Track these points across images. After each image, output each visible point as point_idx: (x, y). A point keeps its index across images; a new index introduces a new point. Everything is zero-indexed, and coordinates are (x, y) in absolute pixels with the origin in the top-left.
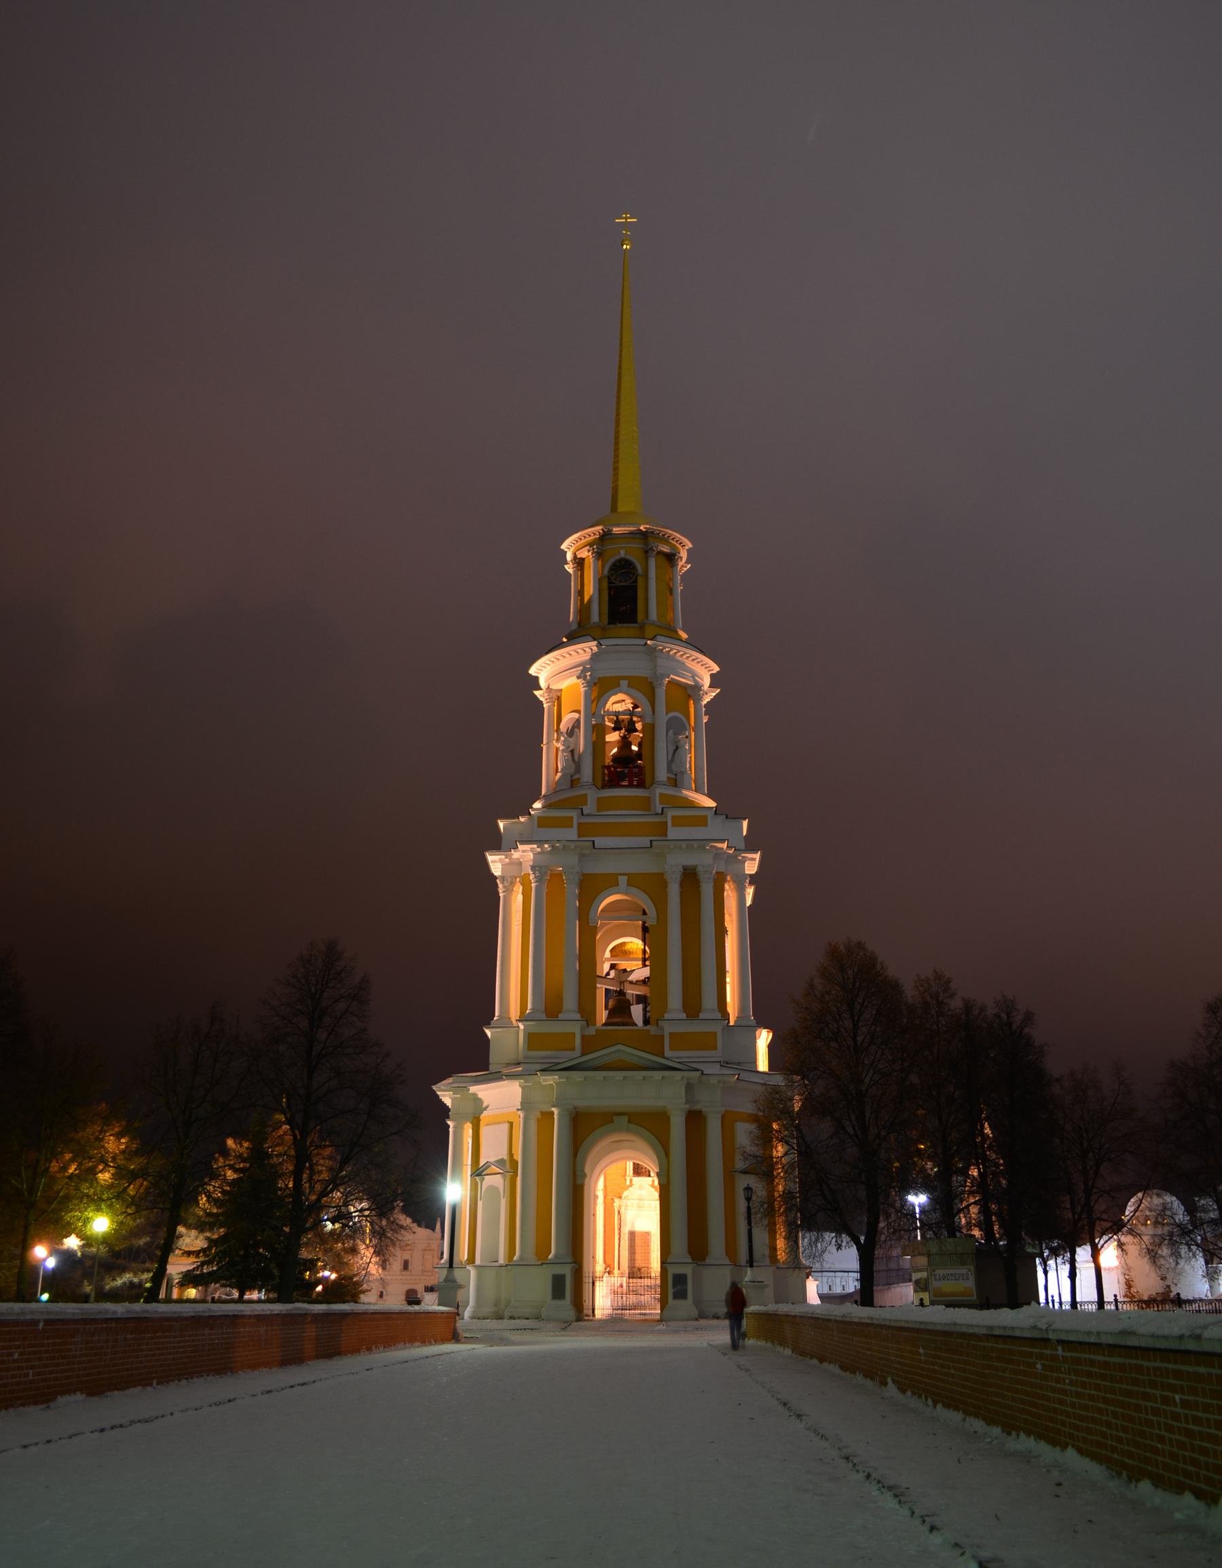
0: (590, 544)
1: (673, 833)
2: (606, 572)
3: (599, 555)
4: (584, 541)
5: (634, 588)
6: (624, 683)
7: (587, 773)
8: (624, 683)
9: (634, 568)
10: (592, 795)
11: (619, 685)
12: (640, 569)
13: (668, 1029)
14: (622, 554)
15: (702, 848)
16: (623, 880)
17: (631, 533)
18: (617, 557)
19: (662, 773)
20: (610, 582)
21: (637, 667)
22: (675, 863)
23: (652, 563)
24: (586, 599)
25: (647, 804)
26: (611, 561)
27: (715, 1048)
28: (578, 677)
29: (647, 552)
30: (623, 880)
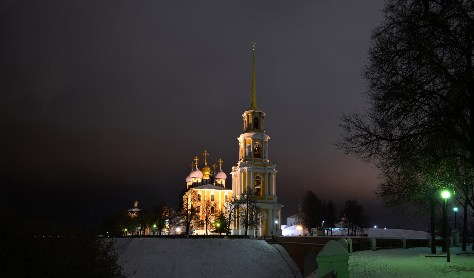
0: (251, 113)
1: (268, 167)
2: (254, 118)
3: (252, 115)
4: (250, 112)
5: (258, 123)
6: (258, 140)
7: (253, 155)
8: (258, 140)
9: (258, 119)
10: (254, 159)
11: (257, 140)
12: (259, 119)
13: (267, 197)
14: (256, 116)
15: (272, 170)
16: (259, 173)
17: (258, 112)
18: (255, 116)
19: (264, 157)
20: (254, 121)
21: (260, 137)
22: (268, 171)
23: (261, 118)
24: (249, 123)
25: (261, 161)
26: (254, 117)
27: (273, 200)
28: (251, 138)
29: (260, 116)
30: (259, 173)
